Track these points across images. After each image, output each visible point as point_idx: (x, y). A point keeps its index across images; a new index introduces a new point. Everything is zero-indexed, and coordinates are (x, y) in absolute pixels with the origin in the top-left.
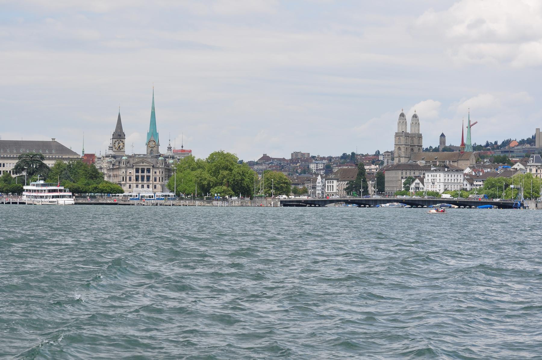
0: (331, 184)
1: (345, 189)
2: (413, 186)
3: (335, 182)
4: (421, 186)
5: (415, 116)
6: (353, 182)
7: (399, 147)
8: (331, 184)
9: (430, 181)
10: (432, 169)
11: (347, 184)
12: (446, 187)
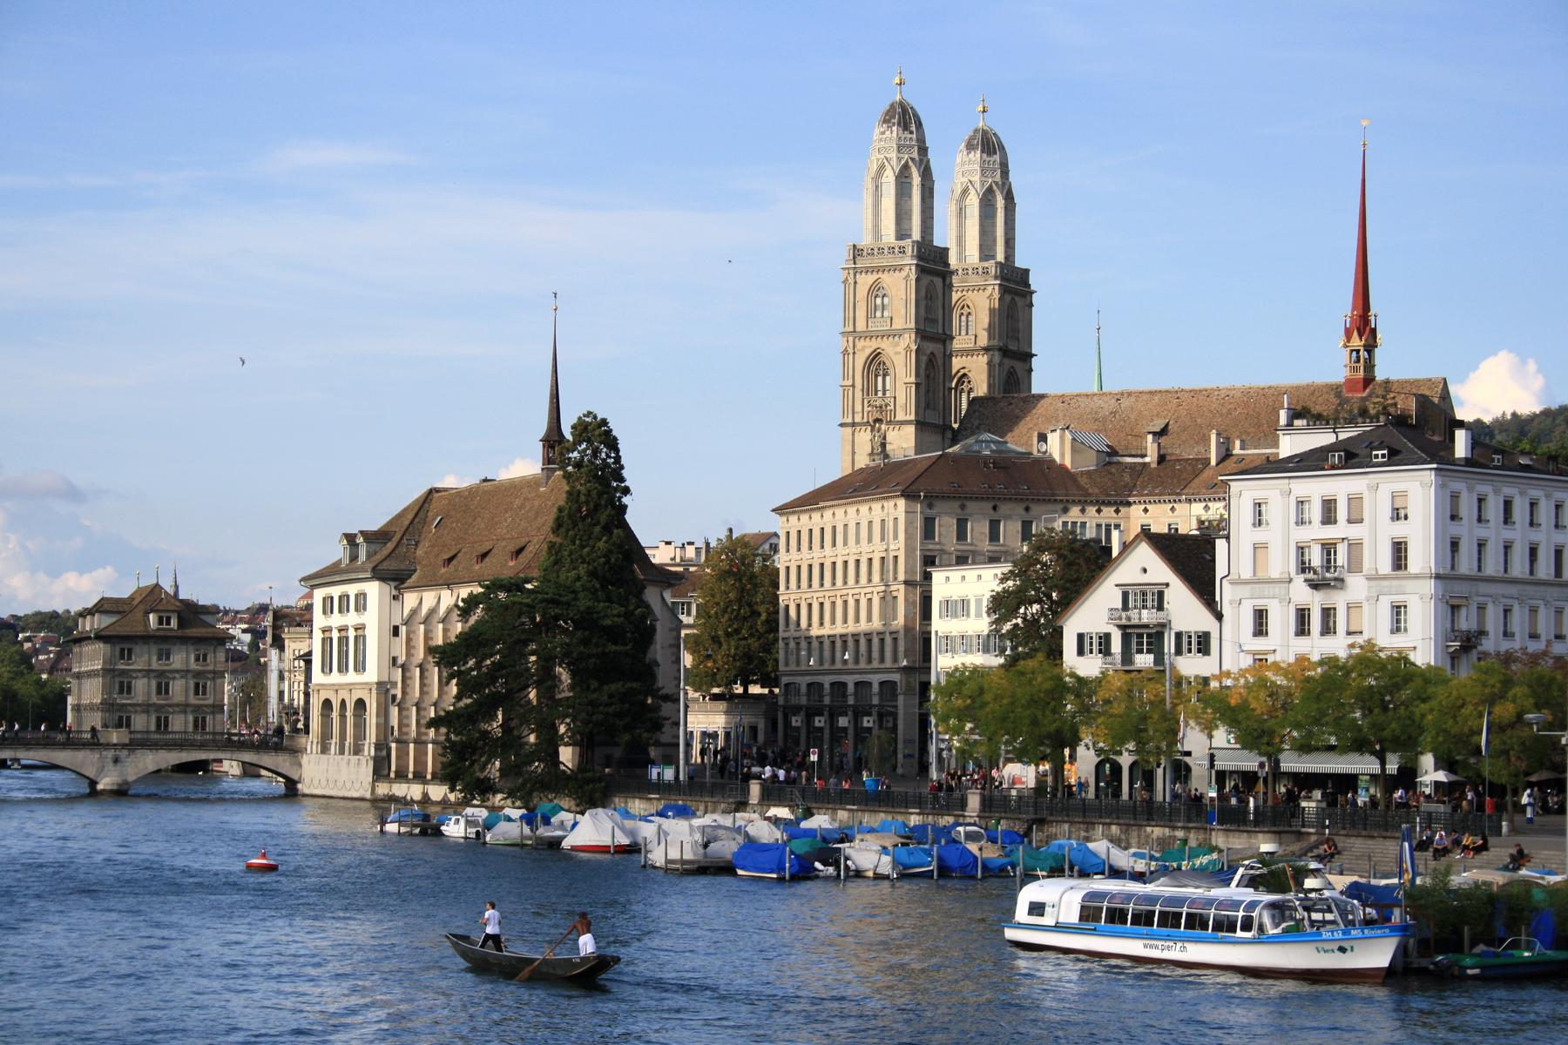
0: (352, 618)
1: (447, 656)
2: (1094, 613)
3: (373, 589)
4: (1184, 609)
5: (988, 144)
6: (514, 586)
7: (875, 359)
8: (352, 618)
9: (1280, 562)
10: (1288, 446)
11: (466, 609)
12: (1466, 622)
